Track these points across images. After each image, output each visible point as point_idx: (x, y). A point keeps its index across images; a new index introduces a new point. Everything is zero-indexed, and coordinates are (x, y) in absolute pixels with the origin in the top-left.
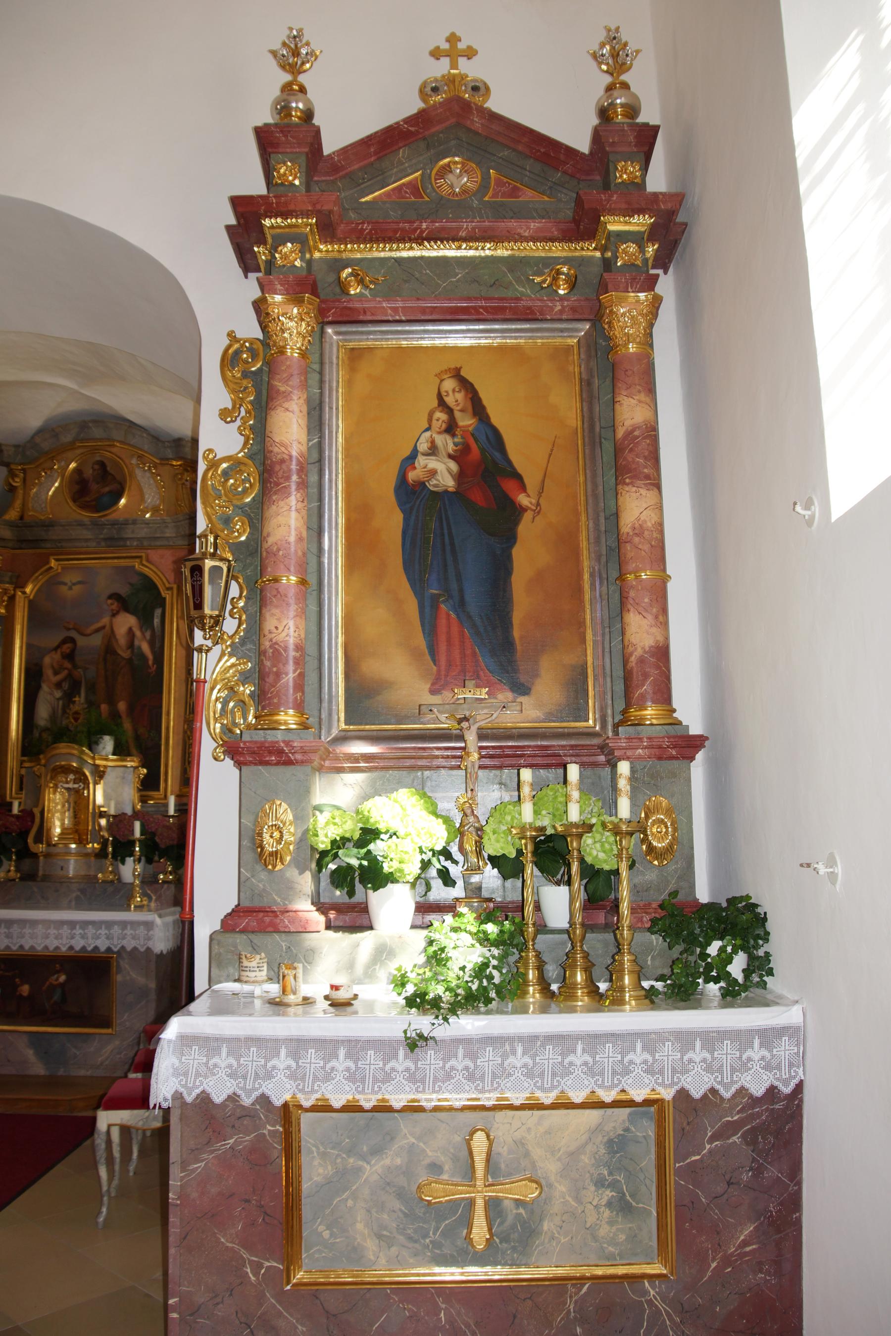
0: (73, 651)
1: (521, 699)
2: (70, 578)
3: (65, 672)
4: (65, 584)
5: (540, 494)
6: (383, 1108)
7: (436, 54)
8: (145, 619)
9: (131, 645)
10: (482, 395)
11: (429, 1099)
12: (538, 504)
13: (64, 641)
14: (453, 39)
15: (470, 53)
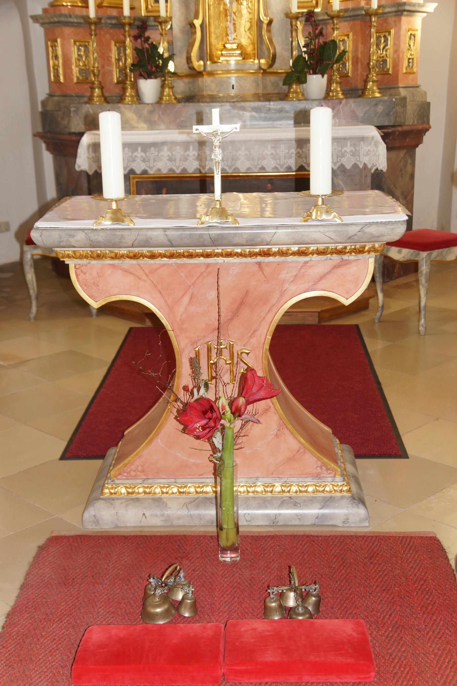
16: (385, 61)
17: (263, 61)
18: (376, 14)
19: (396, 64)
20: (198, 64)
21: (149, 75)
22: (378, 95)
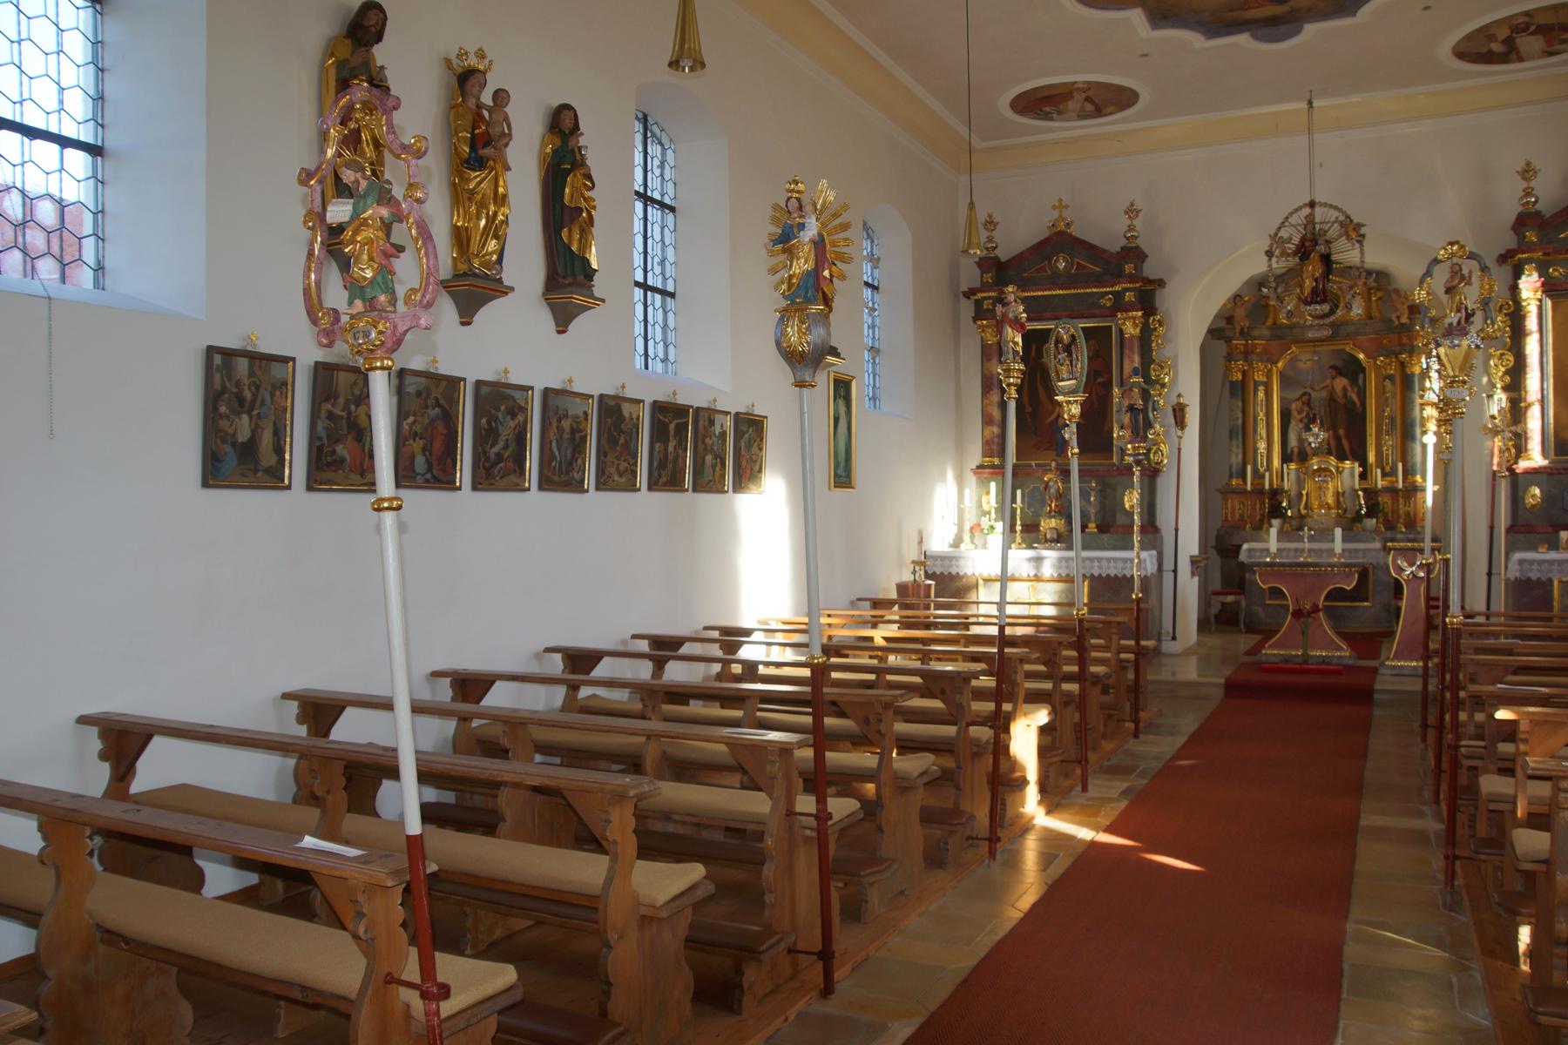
0: (1309, 401)
8: (1353, 380)
13: (1304, 394)
16: (1409, 514)
17: (1340, 511)
18: (1401, 490)
19: (1415, 514)
20: (1304, 512)
21: (1276, 517)
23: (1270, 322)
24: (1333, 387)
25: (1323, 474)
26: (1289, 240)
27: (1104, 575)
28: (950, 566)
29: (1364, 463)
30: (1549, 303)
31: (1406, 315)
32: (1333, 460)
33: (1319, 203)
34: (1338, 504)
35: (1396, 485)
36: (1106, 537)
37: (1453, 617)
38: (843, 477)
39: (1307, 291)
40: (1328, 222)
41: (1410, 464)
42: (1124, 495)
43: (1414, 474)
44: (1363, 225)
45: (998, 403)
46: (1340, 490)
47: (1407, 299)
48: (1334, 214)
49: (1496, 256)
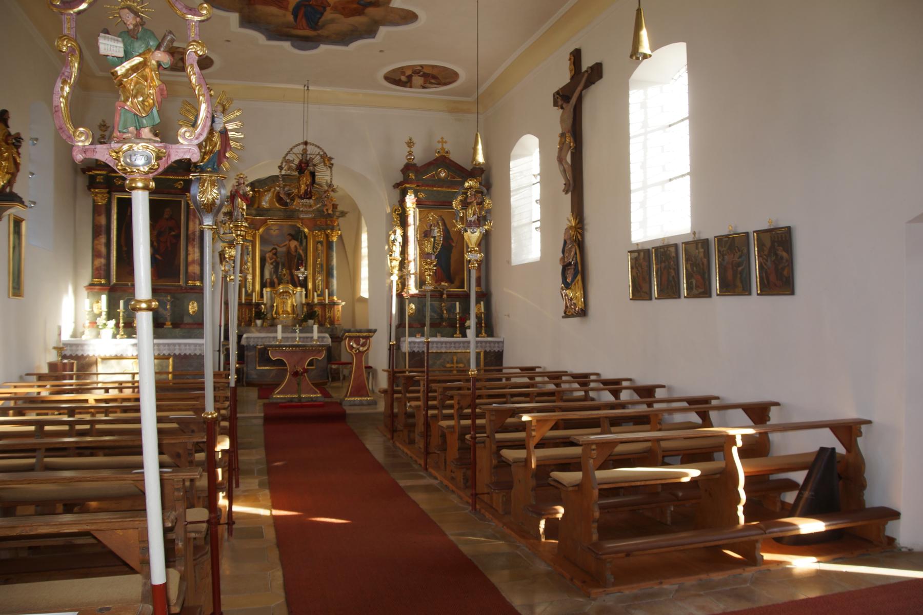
1: (453, 285)
2: (274, 228)
3: (274, 260)
4: (272, 229)
5: (457, 243)
6: (441, 353)
7: (439, 142)
9: (296, 251)
10: (446, 221)
11: (448, 351)
12: (456, 246)
14: (442, 138)
15: (446, 142)
16: (330, 317)
19: (334, 318)
20: (275, 316)
21: (259, 319)
22: (329, 326)
23: (256, 206)
24: (289, 245)
25: (285, 294)
26: (292, 162)
27: (182, 354)
28: (77, 350)
29: (306, 290)
30: (418, 210)
31: (331, 209)
32: (291, 287)
33: (310, 143)
34: (293, 311)
35: (323, 301)
36: (177, 330)
37: (472, 371)
38: (17, 289)
39: (302, 191)
40: (314, 154)
41: (331, 290)
42: (189, 305)
43: (333, 296)
44: (333, 159)
45: (105, 243)
46: (295, 304)
47: (332, 200)
48: (317, 150)
49: (394, 183)
